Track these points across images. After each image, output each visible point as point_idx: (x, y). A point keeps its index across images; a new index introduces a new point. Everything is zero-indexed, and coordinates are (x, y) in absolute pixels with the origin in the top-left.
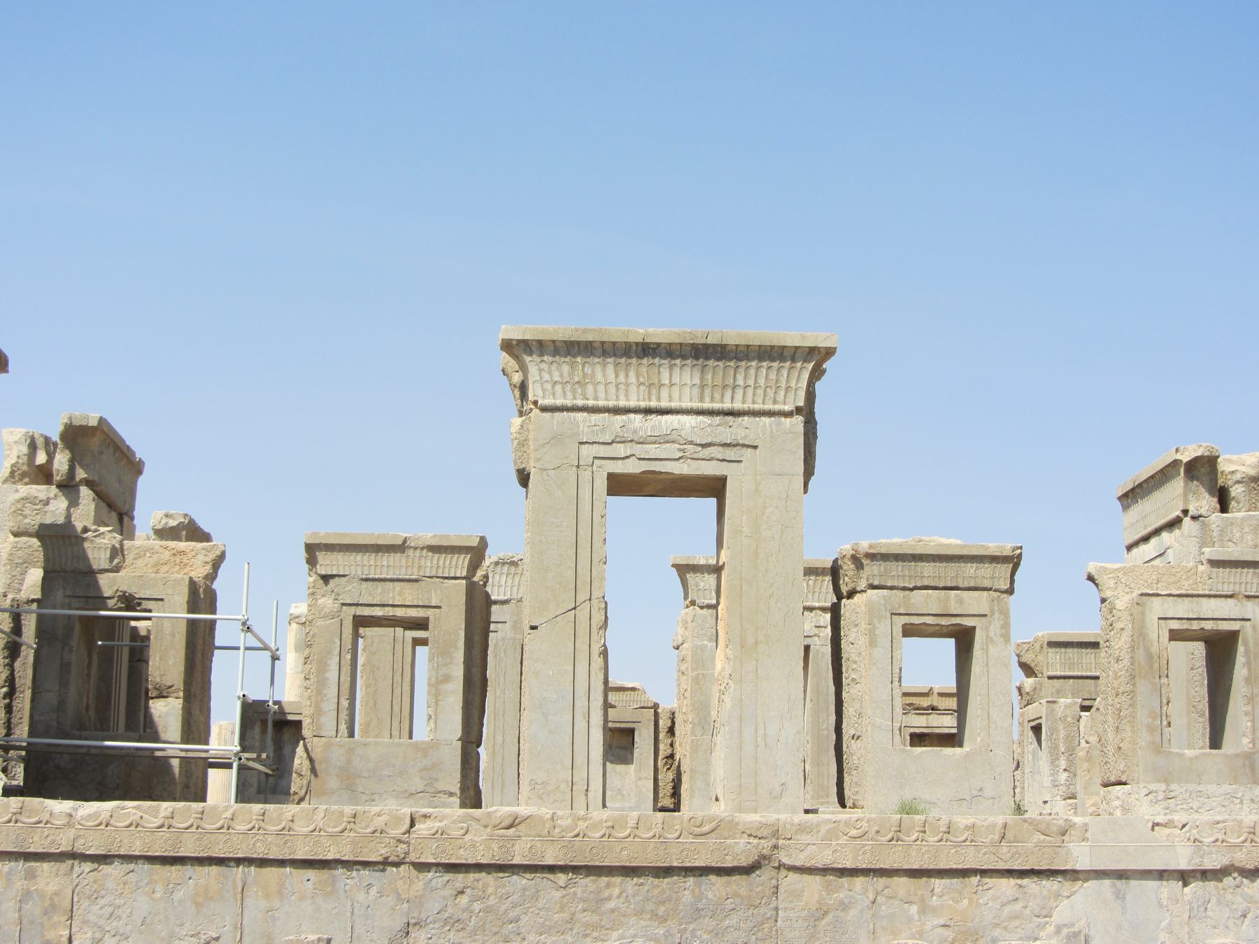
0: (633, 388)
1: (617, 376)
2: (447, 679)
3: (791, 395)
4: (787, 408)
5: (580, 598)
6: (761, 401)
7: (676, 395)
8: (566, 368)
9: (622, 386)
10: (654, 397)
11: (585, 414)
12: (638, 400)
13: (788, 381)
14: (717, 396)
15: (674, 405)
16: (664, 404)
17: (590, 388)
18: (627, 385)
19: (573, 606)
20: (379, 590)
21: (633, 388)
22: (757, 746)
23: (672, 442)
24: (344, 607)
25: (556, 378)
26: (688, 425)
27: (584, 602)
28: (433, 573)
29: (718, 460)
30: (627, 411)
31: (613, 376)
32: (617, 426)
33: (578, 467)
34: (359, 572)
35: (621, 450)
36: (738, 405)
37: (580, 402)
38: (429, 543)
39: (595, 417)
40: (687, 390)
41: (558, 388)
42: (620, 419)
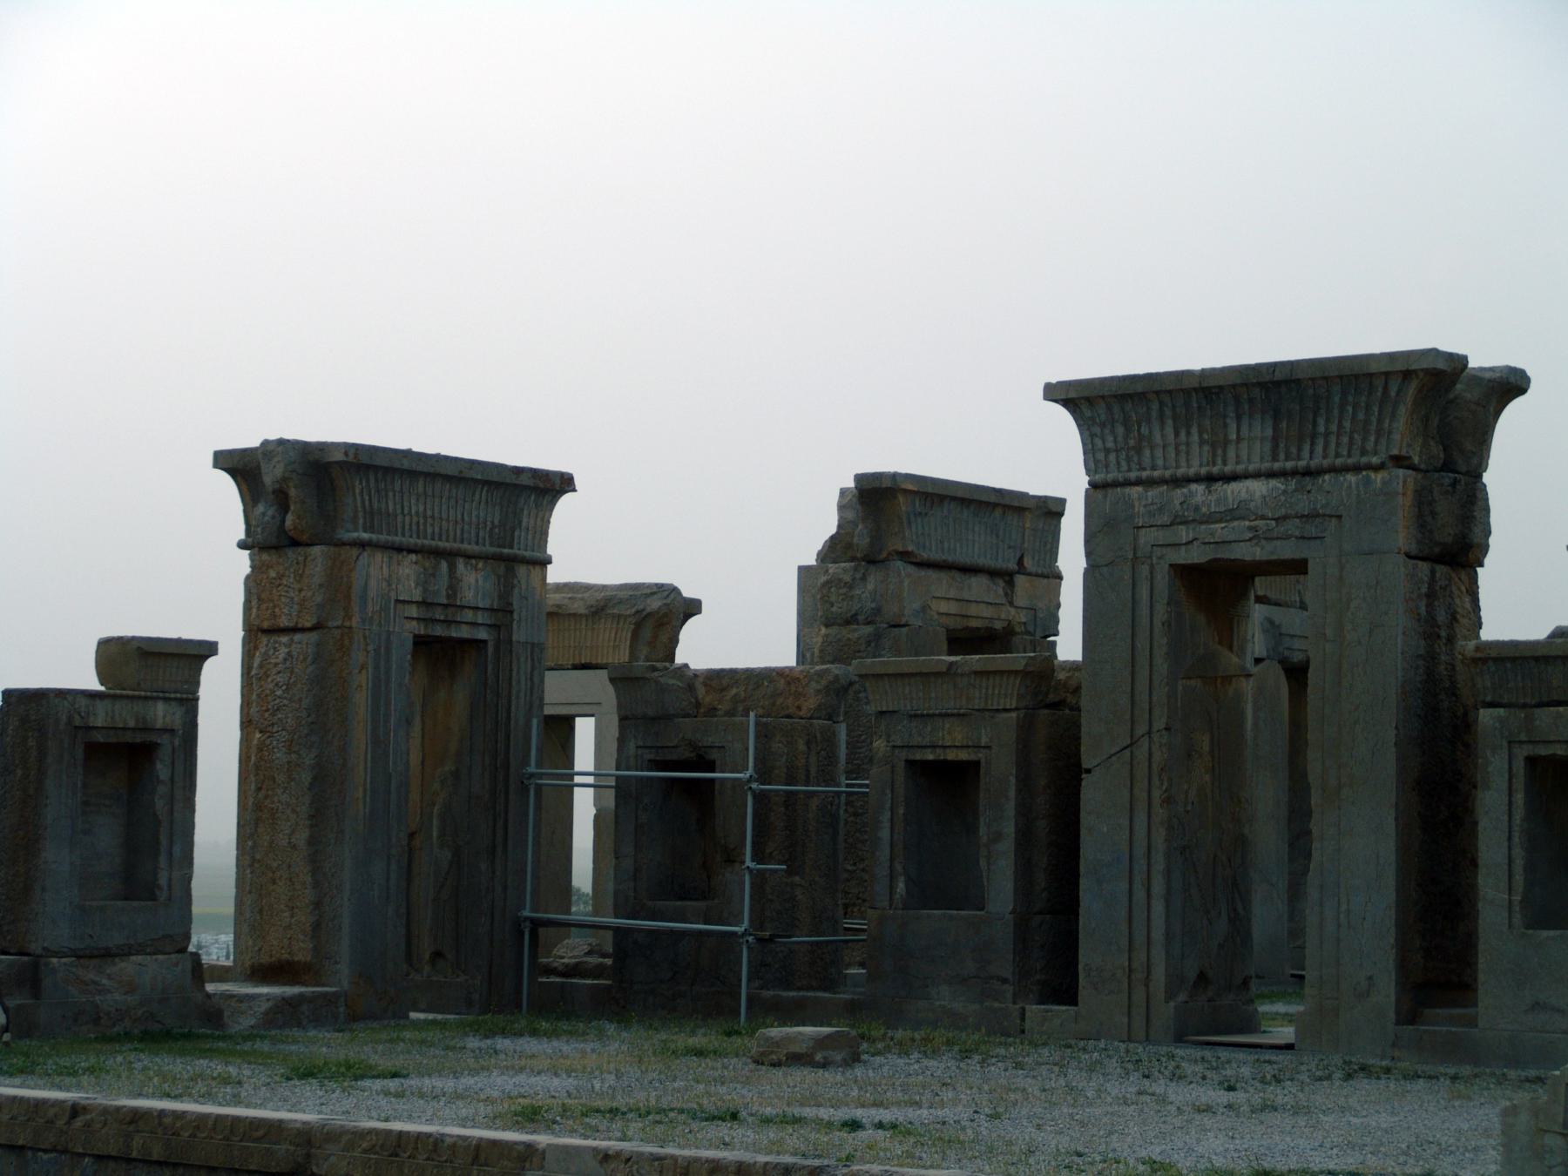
0: (1195, 448)
1: (1177, 434)
2: (998, 837)
3: (1383, 441)
4: (1375, 460)
5: (1141, 729)
6: (1345, 453)
7: (1244, 454)
8: (1120, 430)
9: (1183, 447)
10: (1219, 461)
11: (1140, 489)
12: (1201, 465)
13: (1380, 421)
14: (1294, 450)
15: (1240, 468)
16: (1228, 469)
17: (1147, 453)
18: (1188, 444)
19: (1129, 742)
20: (929, 728)
21: (1195, 448)
22: (1339, 926)
23: (1243, 518)
24: (897, 751)
25: (1110, 445)
26: (1258, 494)
27: (1143, 736)
28: (982, 706)
29: (1297, 538)
30: (1189, 480)
31: (1173, 436)
32: (1177, 502)
33: (1135, 558)
34: (909, 708)
35: (1184, 533)
36: (1316, 462)
37: (1133, 475)
38: (974, 668)
39: (1153, 493)
40: (1258, 445)
41: (1112, 457)
42: (1179, 494)
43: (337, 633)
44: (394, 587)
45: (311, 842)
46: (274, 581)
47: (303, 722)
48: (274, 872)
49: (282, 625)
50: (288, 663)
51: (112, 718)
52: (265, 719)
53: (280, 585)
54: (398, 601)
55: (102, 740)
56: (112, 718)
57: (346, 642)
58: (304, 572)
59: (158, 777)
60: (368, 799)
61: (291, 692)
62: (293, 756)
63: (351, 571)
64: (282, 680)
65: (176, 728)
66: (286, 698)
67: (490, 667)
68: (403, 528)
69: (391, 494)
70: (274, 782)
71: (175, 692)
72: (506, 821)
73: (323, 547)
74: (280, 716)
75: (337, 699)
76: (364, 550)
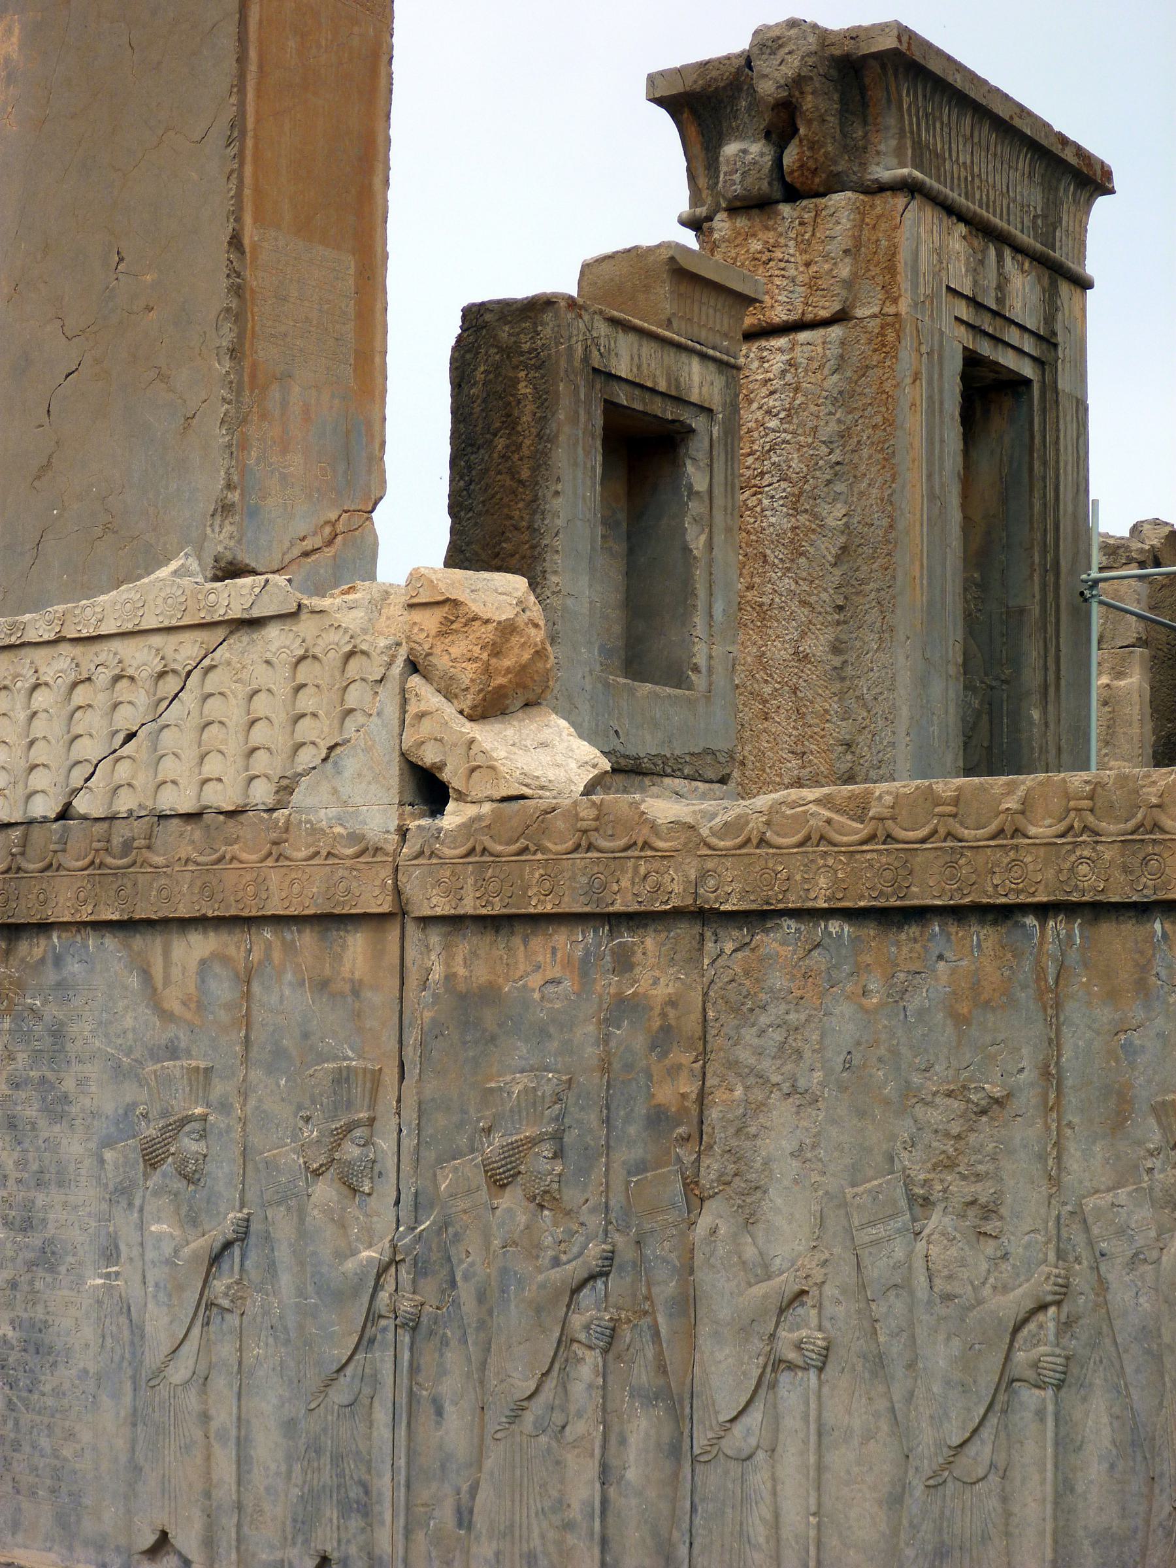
43: (875, 325)
44: (944, 265)
45: (836, 648)
46: (759, 256)
47: (821, 463)
48: (765, 702)
49: (776, 320)
50: (789, 377)
51: (639, 367)
52: (748, 468)
53: (770, 260)
54: (949, 288)
55: (625, 403)
56: (639, 367)
57: (891, 337)
58: (813, 235)
59: (690, 487)
60: (925, 582)
61: (795, 420)
62: (803, 518)
63: (895, 228)
64: (777, 404)
65: (714, 407)
66: (785, 431)
67: (1036, 420)
68: (952, 178)
69: (938, 125)
70: (765, 562)
71: (713, 348)
72: (1058, 650)
73: (849, 194)
74: (775, 459)
75: (875, 427)
76: (913, 198)
